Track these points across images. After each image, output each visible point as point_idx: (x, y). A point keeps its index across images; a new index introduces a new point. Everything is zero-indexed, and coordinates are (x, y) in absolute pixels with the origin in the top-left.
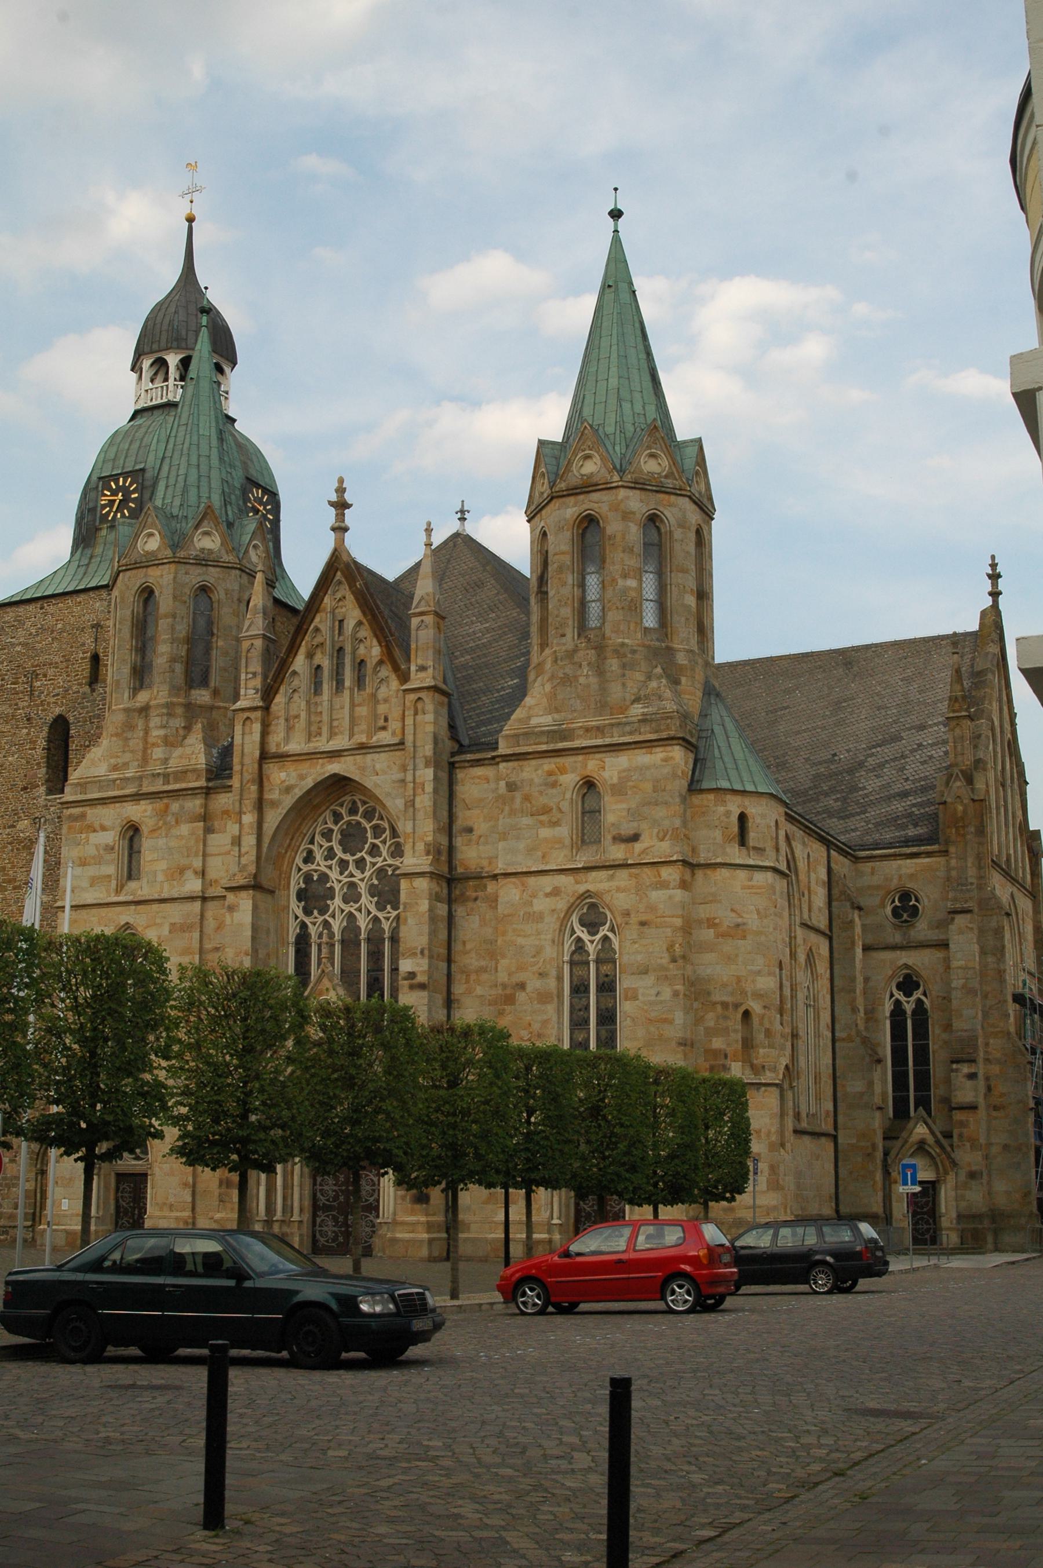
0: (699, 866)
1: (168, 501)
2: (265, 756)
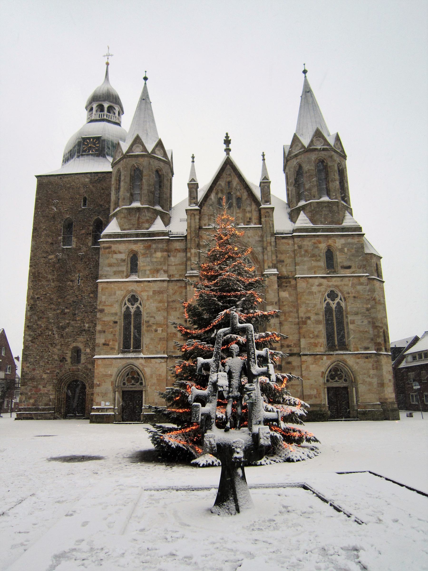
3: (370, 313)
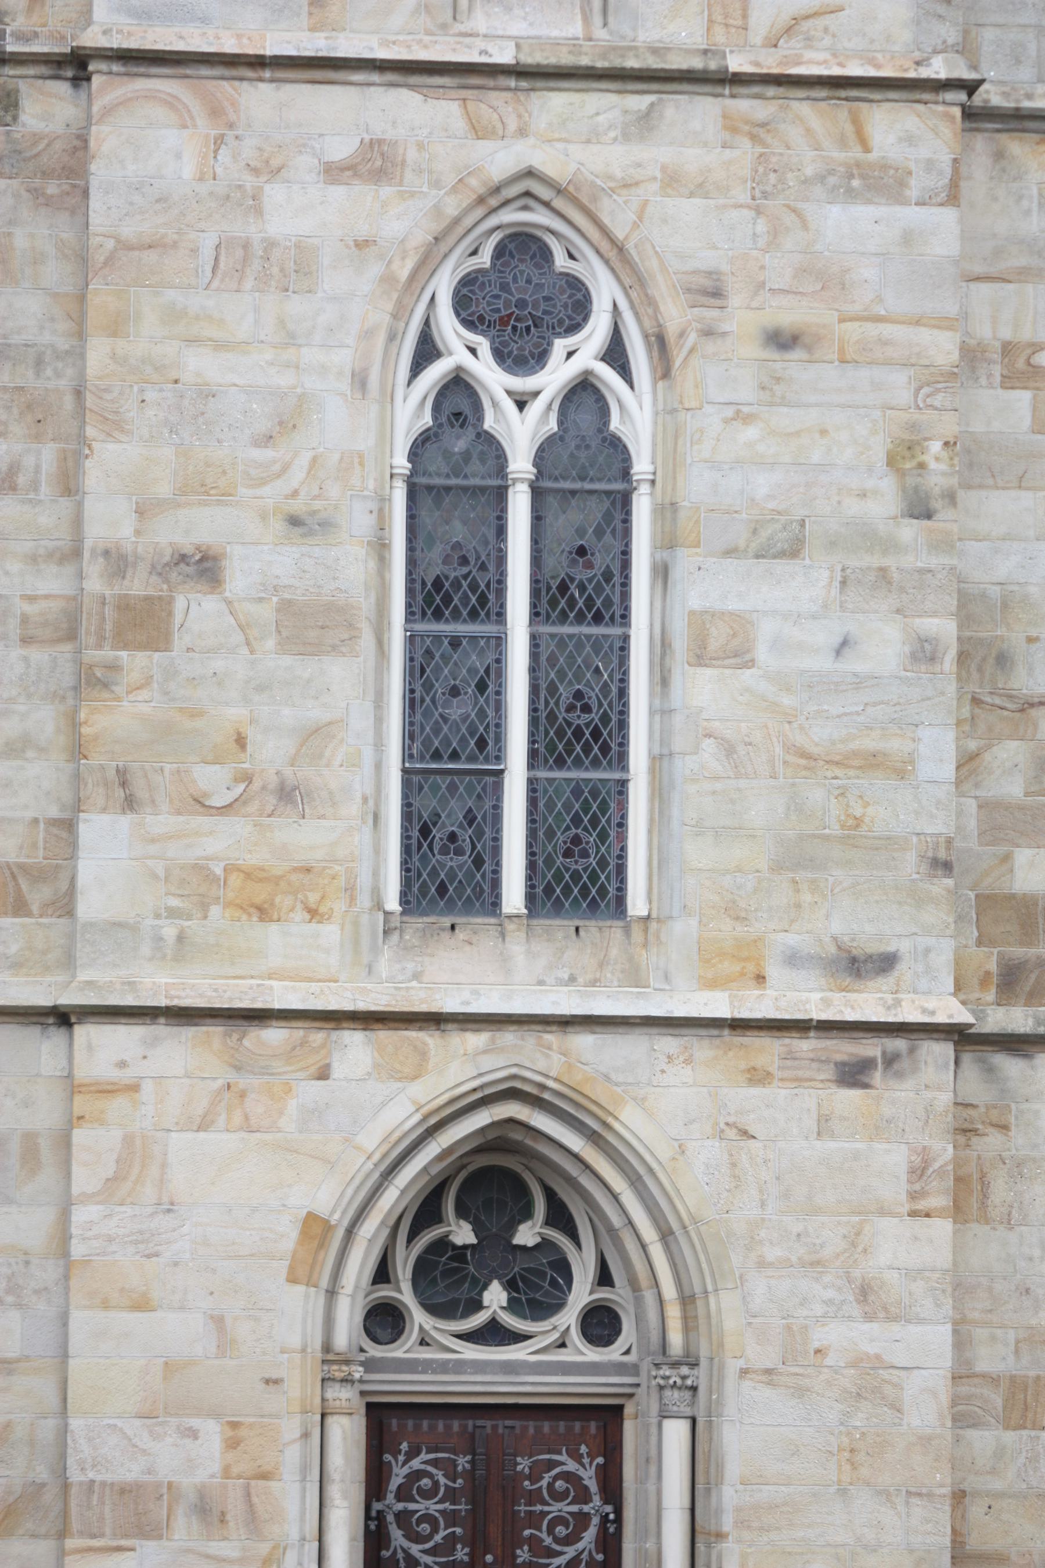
3: (943, 544)
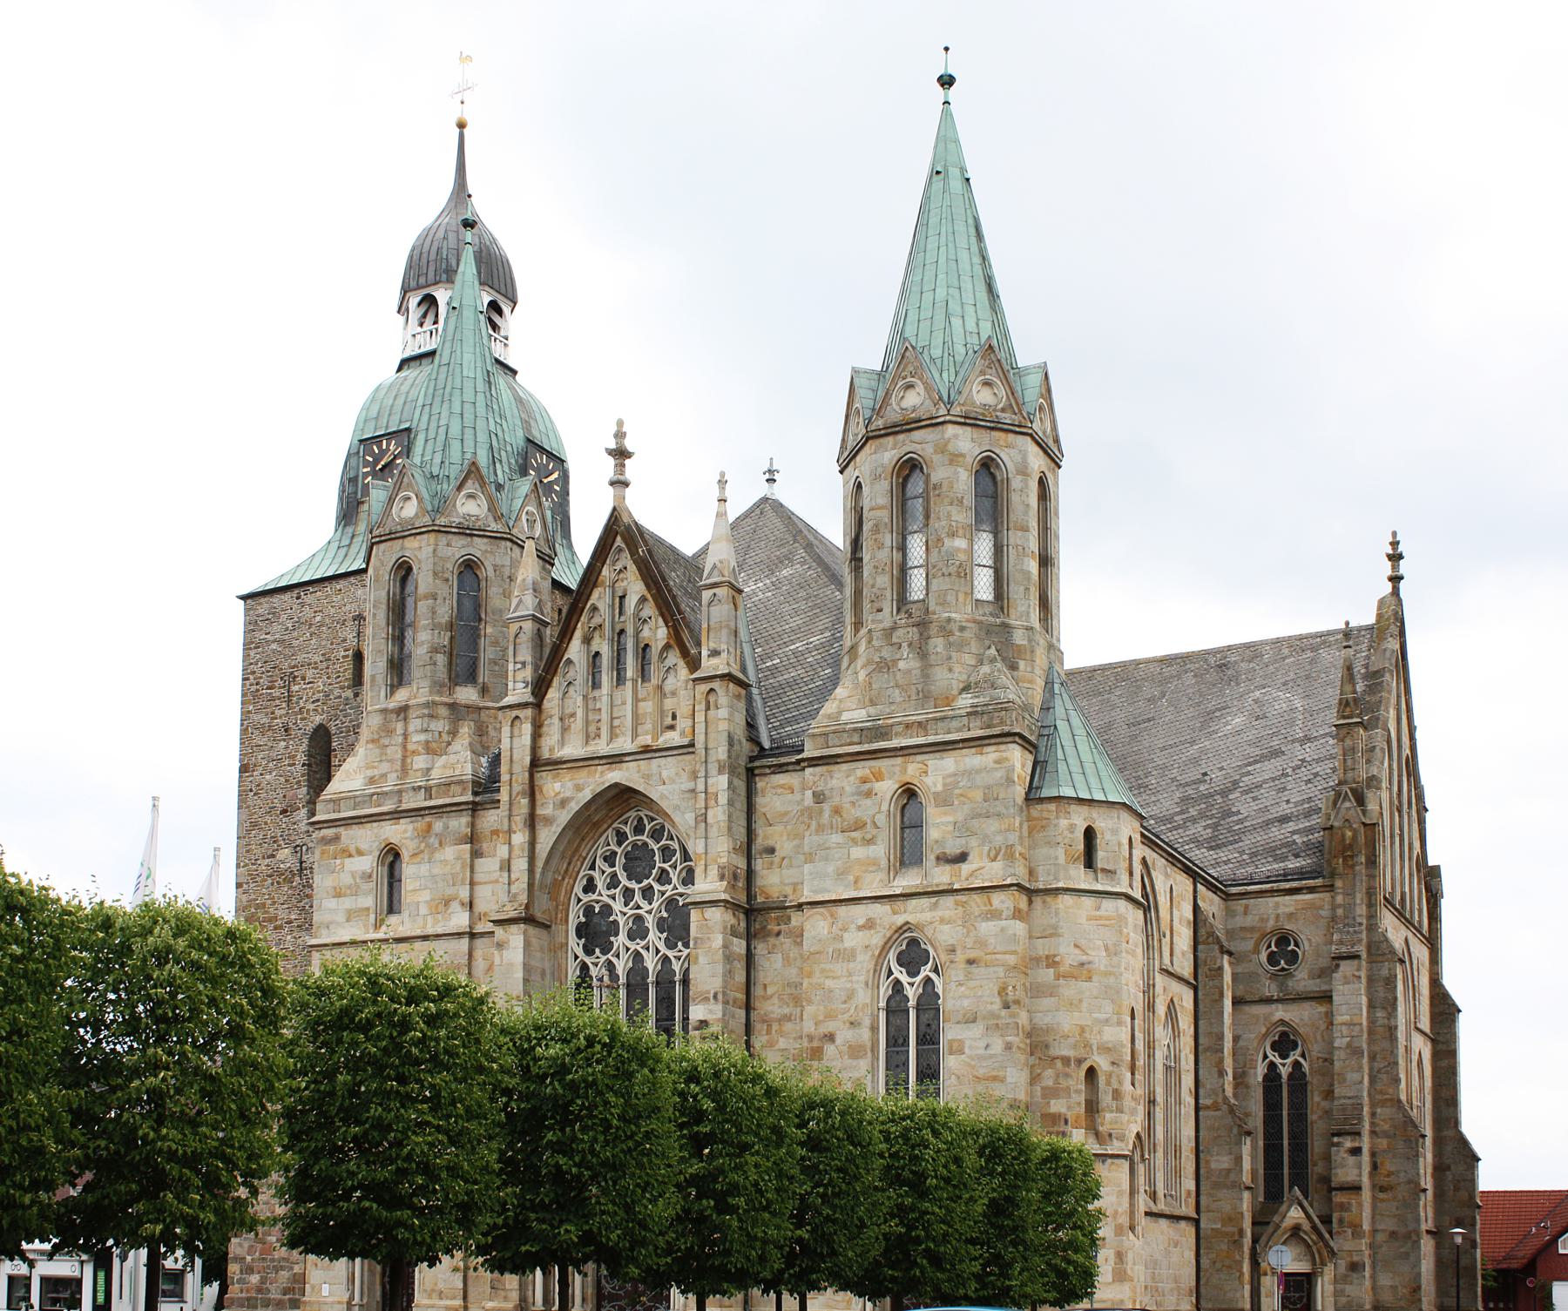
0: (1037, 891)
1: (427, 458)
2: (536, 764)
3: (1013, 1016)
